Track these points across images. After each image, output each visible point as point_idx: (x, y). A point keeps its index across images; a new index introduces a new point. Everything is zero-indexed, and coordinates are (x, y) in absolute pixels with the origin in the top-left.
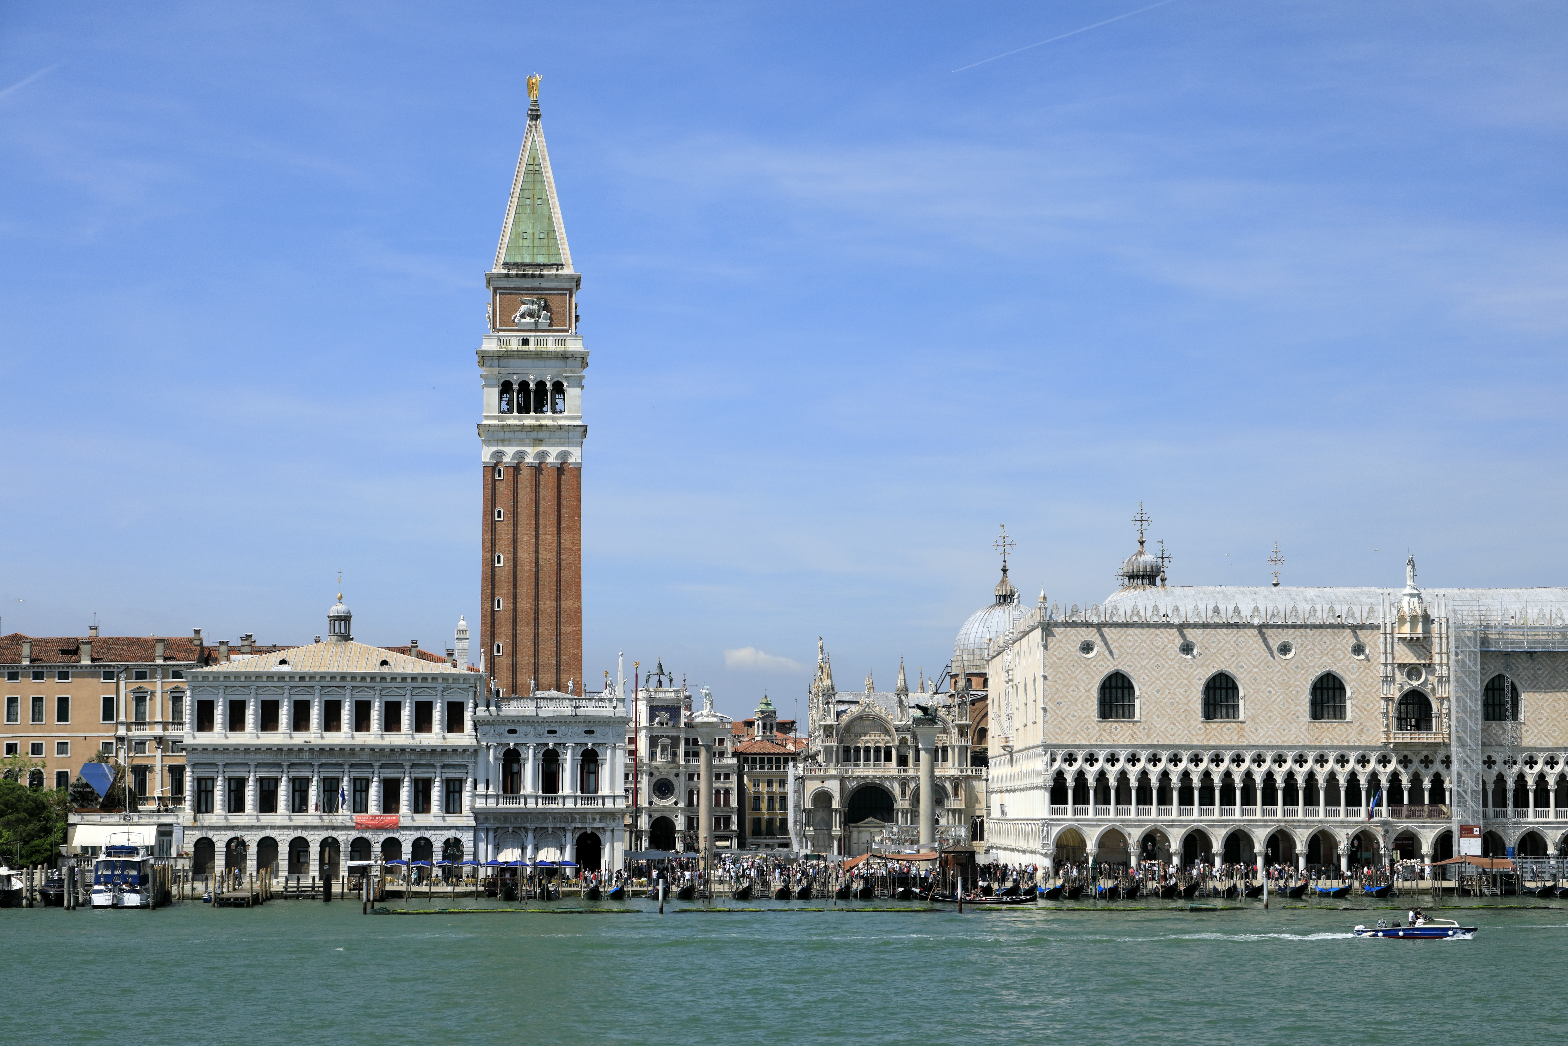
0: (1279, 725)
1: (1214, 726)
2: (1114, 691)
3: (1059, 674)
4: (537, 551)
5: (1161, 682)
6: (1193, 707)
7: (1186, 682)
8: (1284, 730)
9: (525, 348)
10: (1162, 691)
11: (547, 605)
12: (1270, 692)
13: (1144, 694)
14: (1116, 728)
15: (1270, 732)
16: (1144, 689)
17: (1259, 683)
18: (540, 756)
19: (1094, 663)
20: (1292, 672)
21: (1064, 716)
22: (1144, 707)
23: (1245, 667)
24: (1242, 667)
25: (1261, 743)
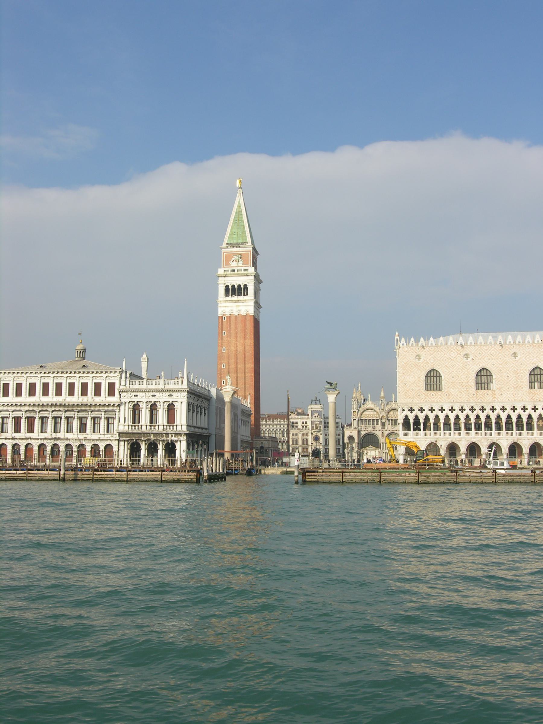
2: (432, 378)
9: (234, 273)
11: (241, 366)
12: (508, 376)
14: (433, 395)
18: (149, 406)
24: (494, 365)
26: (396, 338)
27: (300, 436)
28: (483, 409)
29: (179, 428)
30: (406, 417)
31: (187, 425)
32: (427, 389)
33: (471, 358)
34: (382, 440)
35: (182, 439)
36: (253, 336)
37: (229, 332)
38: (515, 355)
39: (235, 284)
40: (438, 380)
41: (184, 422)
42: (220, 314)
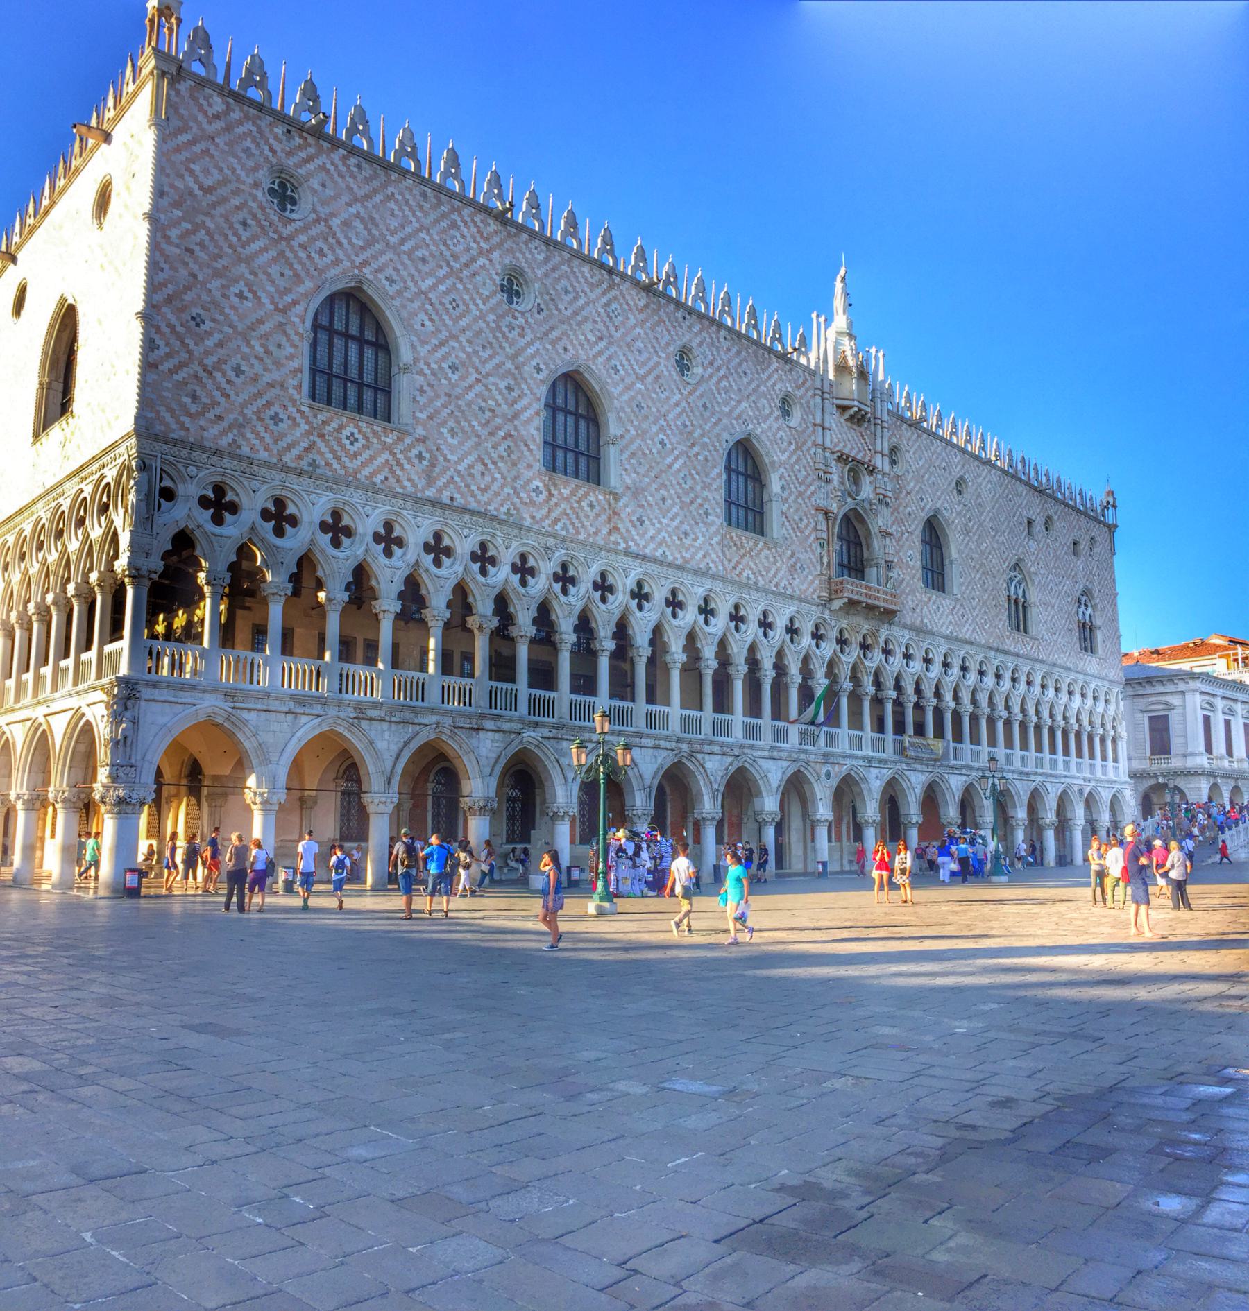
0: (677, 521)
1: (565, 492)
6: (524, 433)
7: (509, 365)
10: (462, 371)
12: (662, 443)
13: (422, 365)
14: (352, 439)
15: (663, 534)
16: (423, 351)
17: (646, 417)
19: (303, 238)
21: (210, 361)
22: (422, 400)
23: (622, 372)
25: (647, 551)
40: (368, 365)
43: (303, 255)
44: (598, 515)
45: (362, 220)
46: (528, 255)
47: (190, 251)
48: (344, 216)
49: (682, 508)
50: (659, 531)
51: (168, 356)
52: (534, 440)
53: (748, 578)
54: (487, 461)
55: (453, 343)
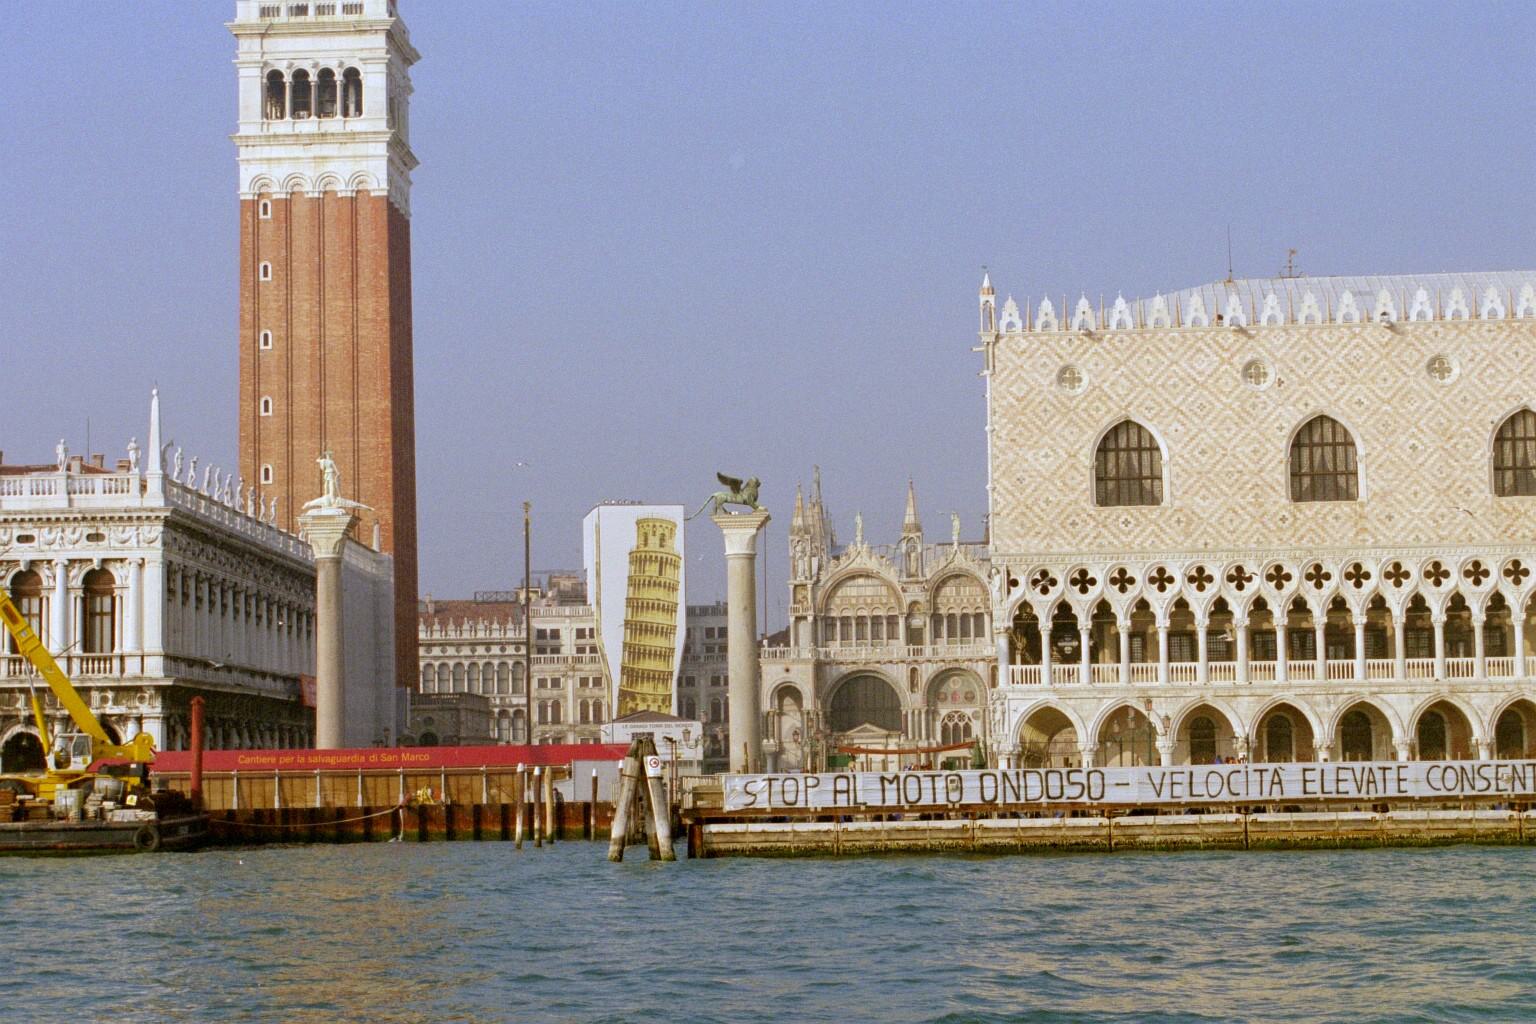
1: (1309, 513)
3: (1020, 428)
4: (321, 325)
5: (1210, 436)
6: (1269, 480)
7: (1254, 434)
8: (1443, 516)
9: (301, 19)
10: (1210, 453)
11: (338, 405)
14: (1126, 523)
17: (1394, 431)
19: (1084, 405)
20: (1454, 408)
21: (1029, 502)
22: (1178, 482)
24: (1360, 403)
26: (983, 299)
27: (570, 686)
28: (1318, 576)
29: (132, 667)
30: (1025, 606)
31: (167, 657)
32: (1103, 500)
33: (1271, 378)
34: (912, 702)
35: (144, 709)
36: (385, 284)
37: (287, 267)
38: (1437, 366)
39: (307, 66)
41: (153, 641)
42: (246, 192)
43: (1085, 416)
44: (1344, 524)
45: (1126, 377)
46: (1268, 346)
47: (1013, 440)
48: (1112, 378)
49: (1438, 496)
50: (1411, 521)
51: (1004, 507)
52: (1278, 481)
53: (1524, 536)
54: (1237, 508)
55: (1204, 435)
